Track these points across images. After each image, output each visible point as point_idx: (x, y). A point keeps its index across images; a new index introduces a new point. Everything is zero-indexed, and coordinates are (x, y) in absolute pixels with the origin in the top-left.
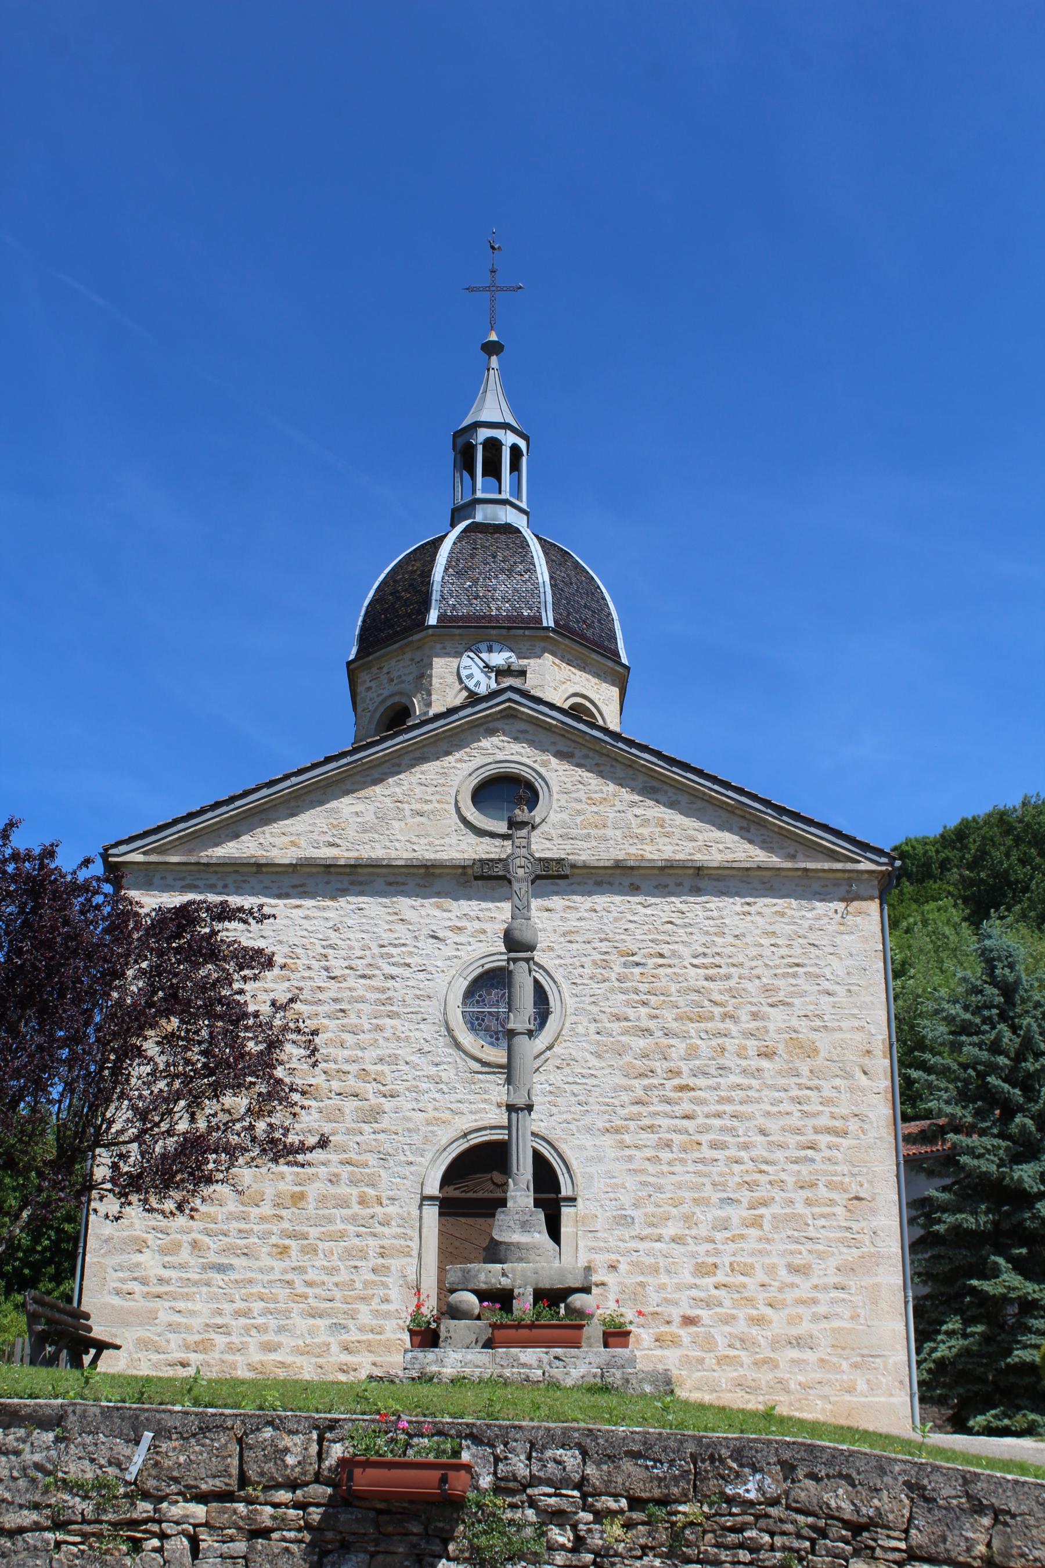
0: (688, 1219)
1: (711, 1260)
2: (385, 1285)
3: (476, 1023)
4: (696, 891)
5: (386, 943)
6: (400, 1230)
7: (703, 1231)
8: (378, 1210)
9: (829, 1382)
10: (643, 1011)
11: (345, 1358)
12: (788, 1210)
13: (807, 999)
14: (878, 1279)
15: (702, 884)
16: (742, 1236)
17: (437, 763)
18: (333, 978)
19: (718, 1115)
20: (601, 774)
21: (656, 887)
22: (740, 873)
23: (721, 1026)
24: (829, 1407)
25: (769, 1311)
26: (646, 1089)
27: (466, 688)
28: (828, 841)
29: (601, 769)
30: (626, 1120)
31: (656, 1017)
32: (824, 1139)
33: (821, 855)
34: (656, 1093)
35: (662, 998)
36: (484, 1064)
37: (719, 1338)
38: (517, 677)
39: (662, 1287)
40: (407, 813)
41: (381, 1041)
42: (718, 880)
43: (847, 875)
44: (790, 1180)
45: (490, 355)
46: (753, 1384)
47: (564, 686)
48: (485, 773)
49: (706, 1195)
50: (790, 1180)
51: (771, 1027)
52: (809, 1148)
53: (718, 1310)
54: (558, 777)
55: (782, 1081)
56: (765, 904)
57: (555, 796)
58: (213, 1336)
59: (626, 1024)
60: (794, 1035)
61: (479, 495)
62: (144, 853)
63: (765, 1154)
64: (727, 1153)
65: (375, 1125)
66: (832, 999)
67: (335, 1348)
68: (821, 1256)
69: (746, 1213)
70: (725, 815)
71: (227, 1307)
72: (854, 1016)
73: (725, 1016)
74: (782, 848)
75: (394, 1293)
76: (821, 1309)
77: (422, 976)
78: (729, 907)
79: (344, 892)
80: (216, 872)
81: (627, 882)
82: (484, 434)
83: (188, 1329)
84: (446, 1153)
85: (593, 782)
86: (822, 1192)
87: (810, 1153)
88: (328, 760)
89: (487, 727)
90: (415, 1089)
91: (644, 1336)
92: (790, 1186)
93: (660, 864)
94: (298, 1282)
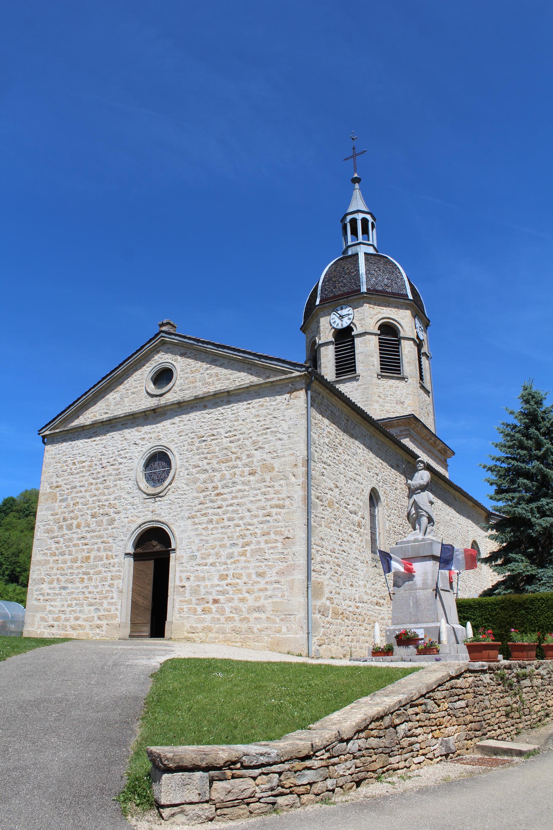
0: (218, 555)
1: (225, 573)
2: (112, 591)
3: (149, 478)
4: (229, 402)
5: (119, 449)
6: (118, 568)
7: (223, 559)
8: (112, 561)
9: (270, 628)
10: (205, 461)
11: (99, 622)
12: (257, 547)
13: (271, 444)
14: (294, 577)
15: (232, 399)
16: (238, 561)
17: (141, 370)
18: (103, 467)
19: (231, 505)
20: (196, 359)
21: (213, 405)
22: (245, 390)
23: (235, 463)
24: (270, 640)
25: (247, 595)
26: (205, 497)
27: (333, 328)
28: (280, 366)
29: (197, 356)
30: (196, 512)
31: (210, 464)
32: (274, 511)
33: (280, 374)
34: (208, 498)
35: (213, 454)
36: (148, 495)
37: (227, 609)
38: (165, 326)
39: (206, 586)
40: (130, 394)
41: (116, 491)
42: (237, 395)
43: (290, 381)
44: (259, 532)
45: (355, 183)
46: (239, 630)
47: (376, 316)
48: (155, 370)
49: (225, 543)
50: (259, 532)
51: (255, 460)
52: (268, 516)
53: (227, 596)
54: (180, 364)
55: (258, 485)
56: (256, 402)
57: (179, 373)
58: (61, 615)
59: (198, 469)
60: (264, 462)
61: (349, 244)
62: (50, 430)
63: (249, 521)
64: (234, 522)
65: (112, 526)
66: (282, 442)
67: (96, 618)
68: (270, 567)
69: (240, 550)
70: (241, 364)
71: (66, 603)
72: (291, 448)
73: (237, 458)
74: (264, 374)
75: (115, 595)
76: (269, 593)
77: (130, 461)
78: (240, 407)
79: (108, 432)
80: (71, 433)
81: (202, 405)
82: (349, 217)
83: (54, 612)
84: (134, 535)
85: (193, 363)
86: (272, 536)
87: (268, 518)
88: (104, 378)
89: (156, 350)
90: (125, 509)
91: (198, 609)
92: (259, 535)
93: (211, 393)
94: (86, 592)
